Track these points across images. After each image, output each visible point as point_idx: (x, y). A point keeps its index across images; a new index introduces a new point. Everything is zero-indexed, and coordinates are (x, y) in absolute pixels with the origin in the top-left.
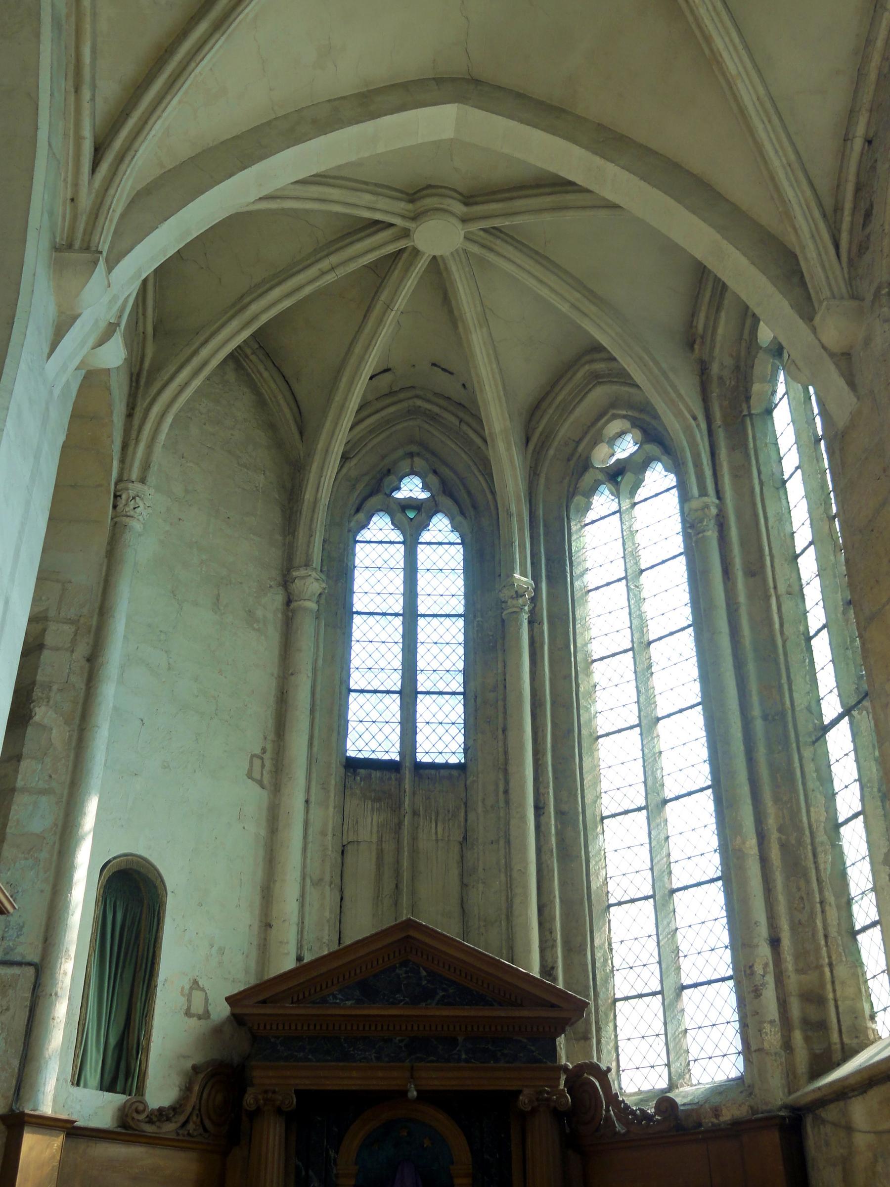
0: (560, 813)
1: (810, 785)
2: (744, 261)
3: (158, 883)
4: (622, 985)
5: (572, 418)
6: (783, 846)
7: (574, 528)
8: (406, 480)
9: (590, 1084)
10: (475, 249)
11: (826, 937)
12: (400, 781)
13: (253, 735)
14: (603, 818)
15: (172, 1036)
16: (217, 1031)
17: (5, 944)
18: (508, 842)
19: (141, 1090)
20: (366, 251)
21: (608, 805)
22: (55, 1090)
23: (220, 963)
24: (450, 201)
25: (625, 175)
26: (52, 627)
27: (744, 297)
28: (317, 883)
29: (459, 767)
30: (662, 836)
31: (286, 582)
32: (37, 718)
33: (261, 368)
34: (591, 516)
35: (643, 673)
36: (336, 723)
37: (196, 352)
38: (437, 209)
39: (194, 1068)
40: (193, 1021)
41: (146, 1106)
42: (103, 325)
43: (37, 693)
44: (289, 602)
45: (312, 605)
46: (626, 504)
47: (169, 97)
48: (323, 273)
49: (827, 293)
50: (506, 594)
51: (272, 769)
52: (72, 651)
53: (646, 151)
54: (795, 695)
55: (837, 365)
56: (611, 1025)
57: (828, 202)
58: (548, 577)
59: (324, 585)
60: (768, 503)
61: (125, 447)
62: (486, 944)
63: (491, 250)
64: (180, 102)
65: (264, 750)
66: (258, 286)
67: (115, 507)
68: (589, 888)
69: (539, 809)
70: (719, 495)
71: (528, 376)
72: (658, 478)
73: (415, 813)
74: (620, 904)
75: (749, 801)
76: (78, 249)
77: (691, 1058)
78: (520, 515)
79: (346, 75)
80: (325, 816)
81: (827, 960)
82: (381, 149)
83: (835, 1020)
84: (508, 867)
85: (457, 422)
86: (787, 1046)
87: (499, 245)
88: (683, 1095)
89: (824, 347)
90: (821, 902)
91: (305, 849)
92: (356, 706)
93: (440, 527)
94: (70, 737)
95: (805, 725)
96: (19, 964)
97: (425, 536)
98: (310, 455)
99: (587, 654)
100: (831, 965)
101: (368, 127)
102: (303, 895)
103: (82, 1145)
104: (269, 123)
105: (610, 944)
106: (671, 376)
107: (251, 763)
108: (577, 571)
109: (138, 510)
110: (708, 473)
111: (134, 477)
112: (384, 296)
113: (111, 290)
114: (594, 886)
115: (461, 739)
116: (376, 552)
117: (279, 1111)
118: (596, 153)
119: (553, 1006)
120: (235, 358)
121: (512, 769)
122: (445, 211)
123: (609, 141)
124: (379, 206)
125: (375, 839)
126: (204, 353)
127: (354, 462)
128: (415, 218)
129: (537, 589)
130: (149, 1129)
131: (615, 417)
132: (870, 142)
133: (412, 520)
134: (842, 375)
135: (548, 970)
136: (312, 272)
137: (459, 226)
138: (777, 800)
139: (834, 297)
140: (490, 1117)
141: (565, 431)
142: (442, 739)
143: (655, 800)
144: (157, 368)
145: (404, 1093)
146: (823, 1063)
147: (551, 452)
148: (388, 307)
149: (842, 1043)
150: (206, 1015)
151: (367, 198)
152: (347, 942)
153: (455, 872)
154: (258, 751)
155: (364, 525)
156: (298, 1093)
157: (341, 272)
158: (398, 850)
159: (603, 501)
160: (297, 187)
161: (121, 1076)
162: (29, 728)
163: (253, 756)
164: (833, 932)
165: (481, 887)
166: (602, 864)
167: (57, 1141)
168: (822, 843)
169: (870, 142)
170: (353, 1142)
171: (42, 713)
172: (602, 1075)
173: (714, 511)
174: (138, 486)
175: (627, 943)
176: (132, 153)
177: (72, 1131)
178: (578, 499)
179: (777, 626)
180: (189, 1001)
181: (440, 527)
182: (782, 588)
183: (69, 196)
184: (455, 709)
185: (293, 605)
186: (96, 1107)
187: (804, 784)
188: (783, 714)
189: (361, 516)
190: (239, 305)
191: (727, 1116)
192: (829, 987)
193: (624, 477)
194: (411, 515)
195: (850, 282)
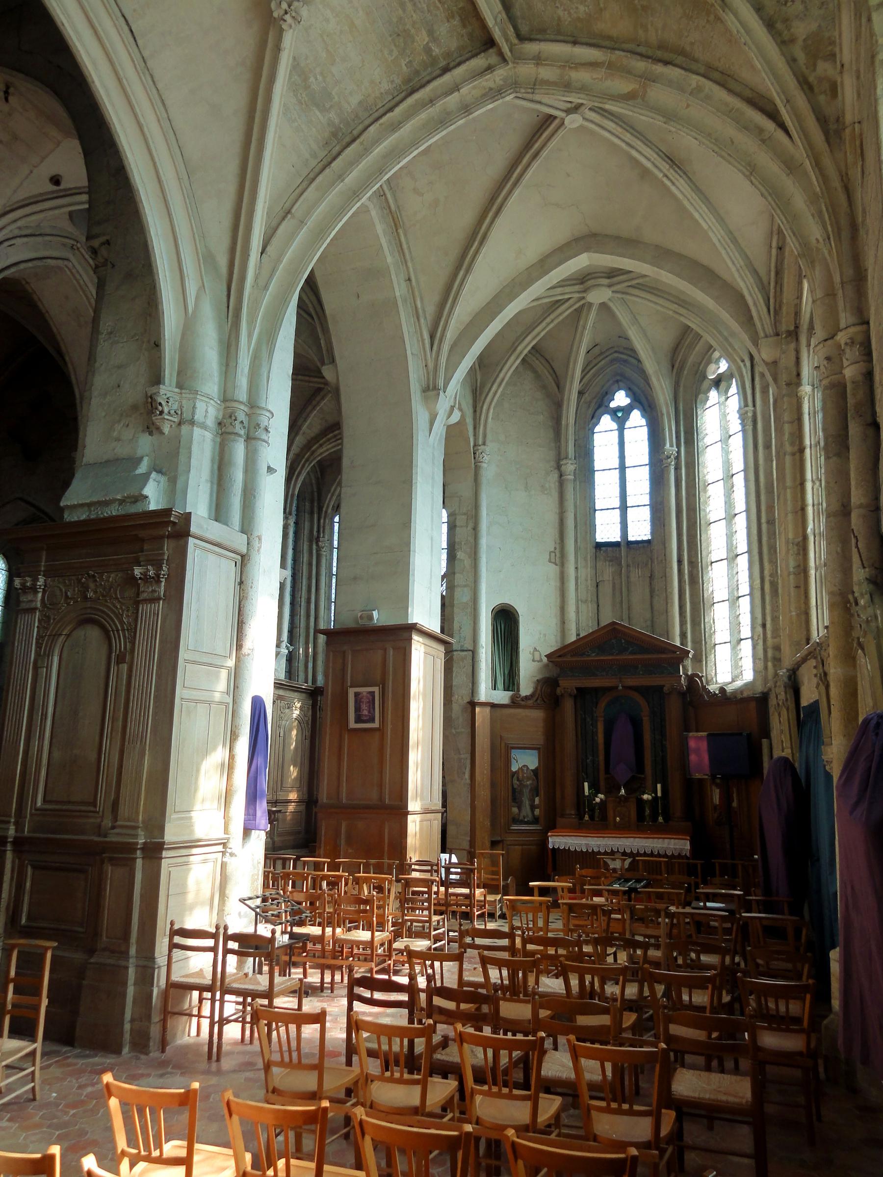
2: (728, 316)
5: (694, 353)
10: (619, 296)
12: (620, 551)
13: (550, 542)
15: (529, 670)
16: (546, 666)
19: (518, 690)
20: (565, 311)
22: (485, 692)
26: (458, 517)
29: (648, 541)
31: (559, 467)
33: (534, 359)
34: (709, 404)
37: (498, 376)
42: (448, 409)
43: (457, 547)
44: (561, 476)
46: (723, 398)
48: (548, 324)
51: (559, 557)
53: (681, 256)
58: (685, 443)
61: (475, 428)
65: (555, 548)
66: (520, 336)
69: (680, 562)
70: (754, 406)
71: (665, 337)
73: (628, 566)
76: (431, 389)
78: (668, 413)
80: (586, 572)
86: (766, 668)
99: (705, 481)
101: (546, 278)
102: (577, 608)
103: (498, 710)
106: (730, 340)
112: (581, 323)
116: (604, 433)
117: (570, 695)
122: (599, 285)
126: (501, 375)
127: (587, 395)
128: (585, 291)
129: (679, 452)
130: (523, 703)
132: (780, 249)
133: (621, 416)
136: (544, 324)
138: (770, 561)
139: (766, 336)
140: (655, 695)
142: (640, 529)
143: (732, 555)
144: (483, 386)
145: (617, 687)
147: (685, 372)
148: (584, 328)
150: (541, 660)
152: (603, 624)
153: (647, 590)
154: (553, 549)
159: (713, 395)
166: (710, 584)
167: (488, 710)
169: (780, 249)
170: (603, 704)
171: (460, 555)
172: (700, 678)
173: (750, 414)
174: (482, 447)
175: (719, 620)
177: (493, 706)
178: (701, 396)
181: (636, 418)
184: (645, 514)
186: (502, 697)
189: (594, 420)
191: (745, 695)
194: (620, 415)
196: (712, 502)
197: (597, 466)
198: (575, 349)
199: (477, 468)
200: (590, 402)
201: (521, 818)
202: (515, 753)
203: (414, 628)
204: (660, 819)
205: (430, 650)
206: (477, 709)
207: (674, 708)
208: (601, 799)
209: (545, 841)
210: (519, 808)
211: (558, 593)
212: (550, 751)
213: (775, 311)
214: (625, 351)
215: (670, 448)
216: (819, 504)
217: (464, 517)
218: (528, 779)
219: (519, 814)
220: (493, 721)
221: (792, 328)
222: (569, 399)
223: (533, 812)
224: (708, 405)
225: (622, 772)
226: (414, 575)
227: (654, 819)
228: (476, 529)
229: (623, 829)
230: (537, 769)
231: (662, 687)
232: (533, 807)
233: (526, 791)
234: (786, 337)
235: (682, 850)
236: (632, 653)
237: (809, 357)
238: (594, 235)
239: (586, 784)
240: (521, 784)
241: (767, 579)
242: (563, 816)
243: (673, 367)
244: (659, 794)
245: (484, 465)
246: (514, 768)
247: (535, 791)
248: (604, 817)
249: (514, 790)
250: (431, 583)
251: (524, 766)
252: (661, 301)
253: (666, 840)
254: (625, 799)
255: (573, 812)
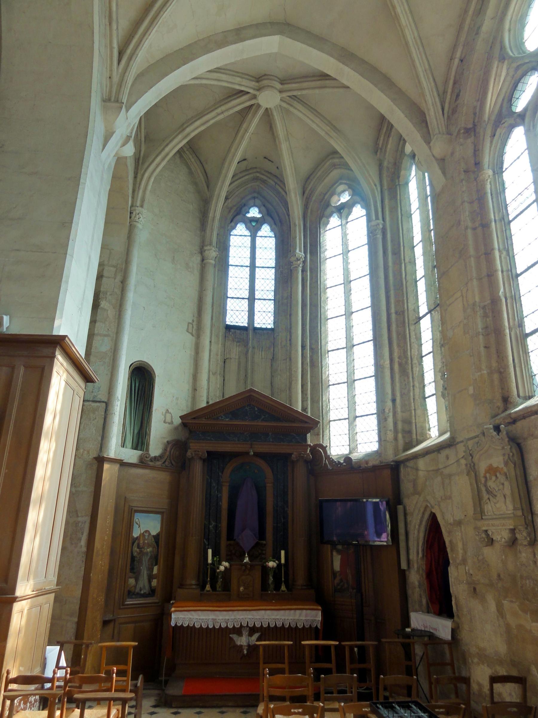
0: (311, 349)
1: (412, 340)
2: (402, 115)
3: (152, 372)
4: (333, 415)
5: (323, 184)
6: (400, 364)
7: (322, 232)
8: (252, 209)
9: (319, 452)
10: (284, 105)
11: (414, 399)
12: (248, 335)
13: (189, 314)
14: (328, 351)
16: (176, 428)
17: (93, 394)
18: (290, 359)
19: (147, 450)
20: (237, 105)
21: (330, 347)
23: (177, 404)
24: (275, 82)
25: (352, 73)
26: (106, 268)
27: (401, 132)
28: (214, 374)
29: (272, 329)
30: (352, 359)
31: (202, 251)
32: (102, 306)
33: (191, 157)
34: (329, 227)
35: (348, 293)
36: (223, 311)
37: (163, 149)
38: (268, 86)
39: (168, 442)
40: (167, 425)
41: (149, 455)
42: (125, 137)
43: (101, 295)
44: (203, 260)
45: (213, 262)
47: (151, 28)
48: (219, 114)
49: (437, 131)
50: (293, 259)
51: (197, 329)
52: (115, 279)
53: (363, 62)
54: (409, 304)
55: (438, 164)
56: (328, 430)
57: (441, 89)
59: (217, 253)
60: (404, 223)
61: (134, 191)
62: (281, 399)
63: (291, 106)
64: (156, 31)
67: (130, 217)
68: (322, 378)
69: (303, 347)
70: (384, 219)
72: (358, 211)
73: (253, 348)
74: (334, 385)
75: (387, 346)
76: (113, 101)
77: (358, 443)
79: (230, 19)
80: (217, 348)
81: (413, 408)
82: (245, 56)
83: (415, 430)
84: (290, 369)
85: (274, 184)
86: (396, 439)
87: (295, 104)
88: (355, 456)
89: (433, 156)
90: (413, 386)
91: (209, 361)
92: (230, 304)
93: (266, 230)
94: (116, 314)
95: (412, 317)
96: (100, 402)
97: (260, 233)
98: (211, 197)
99: (325, 285)
100: (415, 410)
101: (239, 46)
104: (196, 42)
105: (329, 400)
107: (188, 326)
108: (322, 250)
109: (140, 219)
110: (380, 210)
111: (138, 204)
112: (244, 126)
113: (127, 121)
114: (324, 378)
115: (272, 318)
116: (239, 239)
117: (201, 458)
118: (340, 62)
119: (306, 422)
120: (180, 152)
121: (293, 331)
122: (272, 87)
123: (346, 56)
124: (243, 84)
125: (237, 357)
126: (167, 149)
127: (230, 200)
128: (259, 89)
129: (306, 257)
131: (341, 184)
133: (254, 226)
134: (441, 169)
135: (304, 409)
137: (278, 94)
138: (399, 346)
141: (320, 189)
142: (265, 318)
144: (146, 156)
145: (247, 453)
146: (409, 445)
148: (246, 131)
149: (417, 439)
150: (172, 423)
151: (238, 80)
152: (227, 396)
154: (191, 321)
155: (234, 228)
156: (208, 452)
157: (226, 114)
158: (247, 362)
159: (334, 221)
160: (208, 73)
161: (140, 445)
162: (99, 310)
163: (189, 323)
164: (417, 397)
165: (279, 376)
167: (116, 467)
168: (415, 364)
169: (462, 61)
170: (228, 471)
171: (103, 304)
172: (324, 448)
173: (381, 226)
174: (140, 209)
175: (336, 400)
176: (135, 56)
177: (122, 464)
178: (324, 219)
179: (404, 276)
180: (165, 417)
181: (266, 230)
182: (407, 260)
183: (108, 76)
184: (270, 306)
185: (205, 261)
186: (131, 455)
187: (410, 340)
188: (403, 312)
189: (233, 224)
190: (182, 128)
191: (370, 464)
192: (413, 418)
193: (344, 210)
194: (254, 224)
195: (447, 127)
196: (329, 302)
197: (231, 261)
198: (233, 150)
199: (131, 228)
200: (231, 208)
201: (137, 590)
202: (138, 517)
203: (60, 342)
204: (283, 588)
205: (71, 381)
206: (106, 466)
207: (300, 476)
208: (226, 568)
209: (163, 616)
210: (137, 580)
211: (192, 361)
212: (172, 518)
213: (451, 113)
214: (264, 173)
215: (299, 253)
216: (508, 271)
217: (113, 269)
218: (149, 545)
219: (135, 587)
220: (120, 480)
221: (470, 126)
222: (219, 195)
223: (150, 582)
224: (328, 228)
225: (247, 538)
226: (67, 282)
227: (277, 587)
228: (124, 282)
229: (247, 599)
230: (158, 535)
231: (291, 454)
232: (151, 577)
233: (145, 560)
234: (464, 133)
235: (313, 621)
236: (263, 420)
237: (490, 147)
238: (289, 25)
239: (210, 551)
240: (141, 551)
241: (396, 360)
242: (182, 586)
243: (304, 193)
244: (283, 561)
245: (140, 226)
246: (136, 534)
247: (155, 560)
248: (226, 587)
249: (133, 558)
250: (82, 304)
251: (146, 531)
252: (317, 121)
253: (298, 612)
254: (251, 567)
255: (194, 582)
